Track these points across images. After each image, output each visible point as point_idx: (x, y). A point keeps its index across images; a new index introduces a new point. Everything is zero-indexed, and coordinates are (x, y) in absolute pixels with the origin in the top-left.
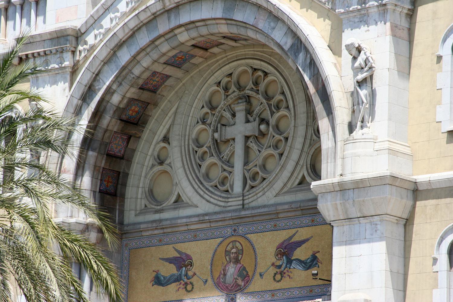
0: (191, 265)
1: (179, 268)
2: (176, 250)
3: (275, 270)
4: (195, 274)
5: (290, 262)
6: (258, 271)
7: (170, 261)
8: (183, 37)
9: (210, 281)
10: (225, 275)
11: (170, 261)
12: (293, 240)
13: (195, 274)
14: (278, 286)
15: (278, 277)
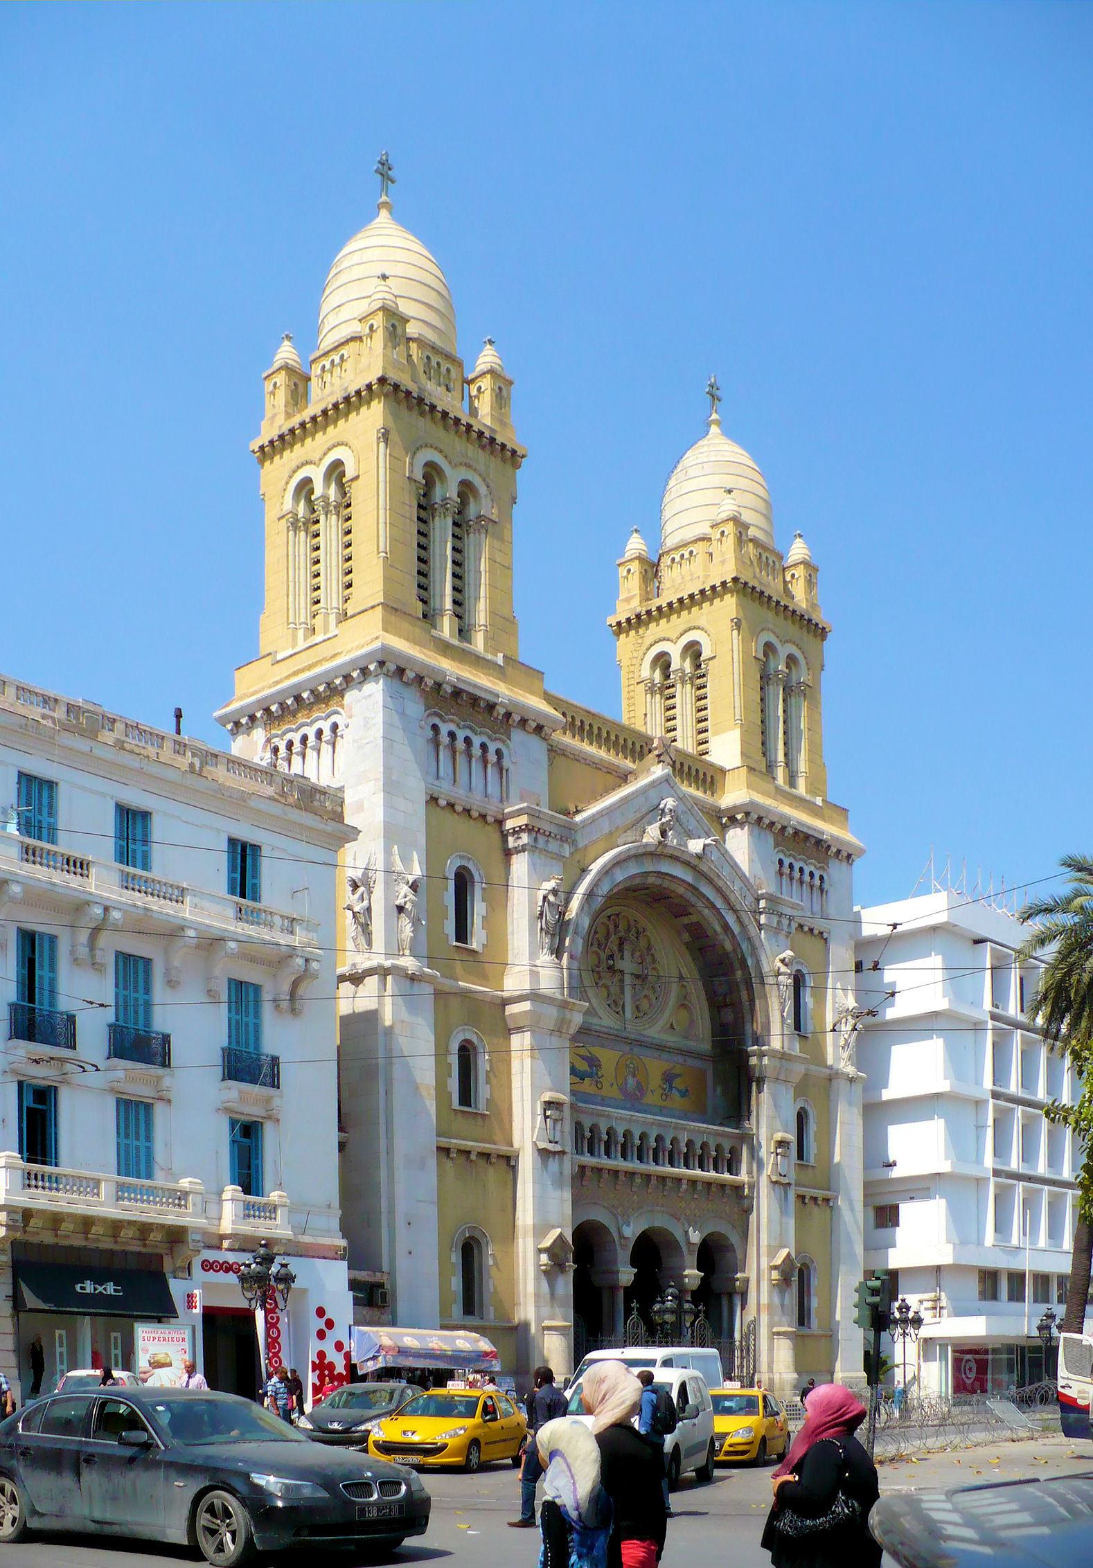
0: (600, 1066)
1: (591, 1066)
2: (589, 1052)
3: (661, 1091)
4: (603, 1076)
5: (671, 1088)
6: (650, 1089)
7: (583, 1058)
8: (651, 880)
9: (615, 1085)
10: (626, 1084)
11: (583, 1058)
12: (673, 1071)
13: (603, 1076)
14: (664, 1104)
15: (664, 1097)
